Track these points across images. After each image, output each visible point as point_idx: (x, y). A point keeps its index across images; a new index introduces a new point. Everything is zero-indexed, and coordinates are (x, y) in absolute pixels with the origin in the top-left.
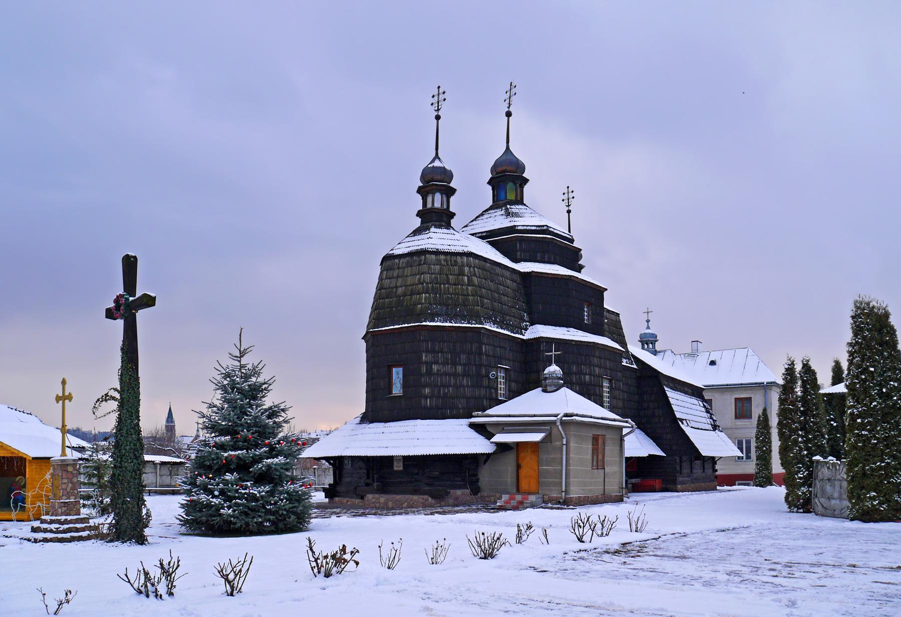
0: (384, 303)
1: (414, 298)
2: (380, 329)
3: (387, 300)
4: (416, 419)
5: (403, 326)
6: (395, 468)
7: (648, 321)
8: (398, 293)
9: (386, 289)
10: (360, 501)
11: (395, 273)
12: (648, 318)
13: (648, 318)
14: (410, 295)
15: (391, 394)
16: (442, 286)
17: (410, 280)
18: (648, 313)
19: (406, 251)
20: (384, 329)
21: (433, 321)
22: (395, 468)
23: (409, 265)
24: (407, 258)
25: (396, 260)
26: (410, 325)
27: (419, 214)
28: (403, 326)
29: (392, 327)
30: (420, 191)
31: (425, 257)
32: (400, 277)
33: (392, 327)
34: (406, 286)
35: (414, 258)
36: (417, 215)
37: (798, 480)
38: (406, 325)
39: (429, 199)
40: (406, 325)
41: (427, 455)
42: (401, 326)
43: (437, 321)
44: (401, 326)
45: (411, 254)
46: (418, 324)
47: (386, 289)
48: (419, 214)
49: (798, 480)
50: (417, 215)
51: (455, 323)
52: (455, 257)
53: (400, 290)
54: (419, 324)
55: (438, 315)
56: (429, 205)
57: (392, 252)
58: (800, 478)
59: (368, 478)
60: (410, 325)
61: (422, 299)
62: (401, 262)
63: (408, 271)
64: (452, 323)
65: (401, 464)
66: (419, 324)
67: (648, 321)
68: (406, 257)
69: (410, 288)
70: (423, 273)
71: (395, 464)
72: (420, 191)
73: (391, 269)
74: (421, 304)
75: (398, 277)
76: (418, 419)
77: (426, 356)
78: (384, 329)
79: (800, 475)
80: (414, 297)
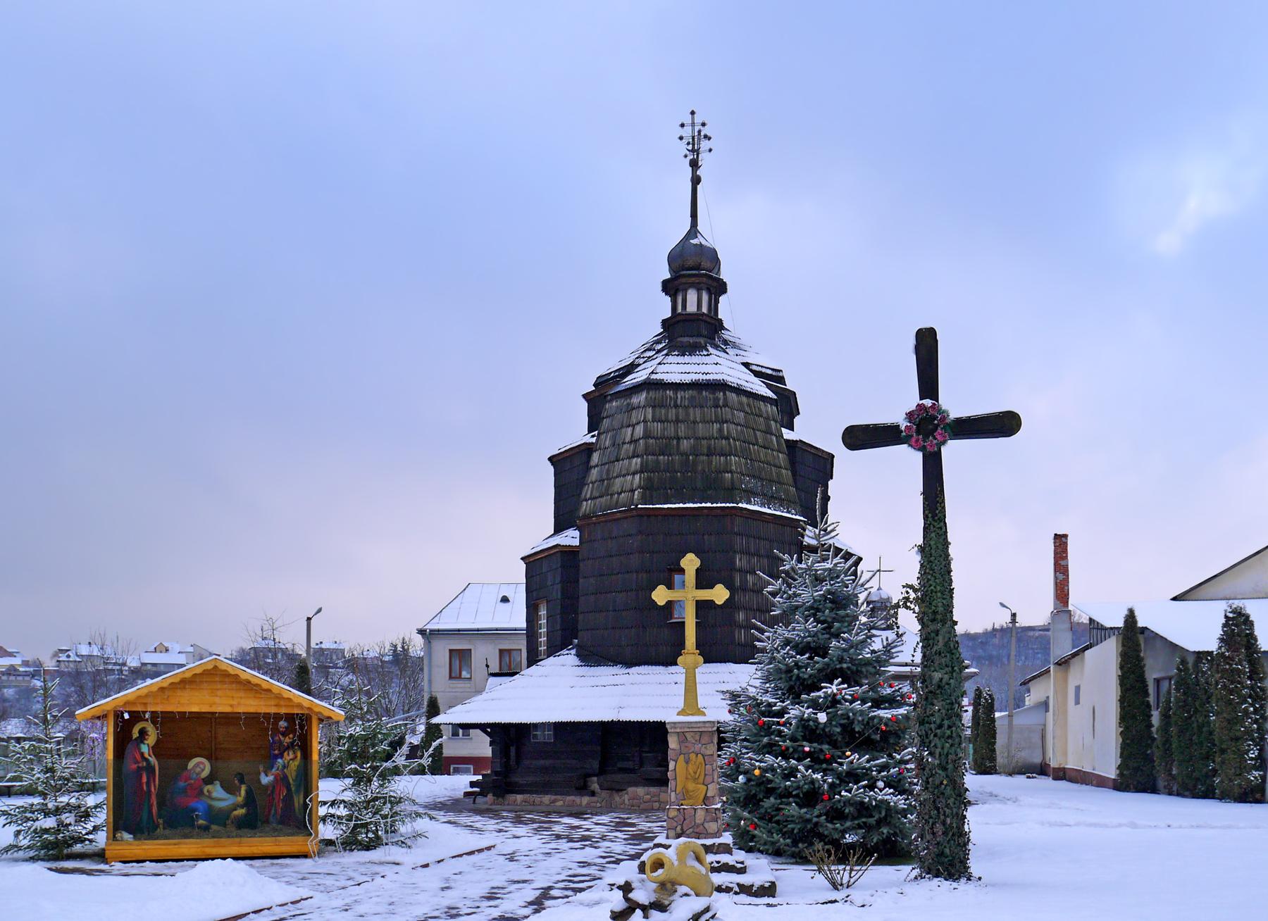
0: (657, 461)
1: (714, 460)
2: (657, 506)
3: (662, 457)
4: (725, 662)
5: (703, 505)
8: (682, 448)
9: (657, 438)
11: (672, 414)
14: (707, 455)
15: (671, 619)
16: (751, 446)
17: (701, 429)
19: (687, 379)
20: (666, 506)
21: (749, 502)
23: (694, 404)
24: (690, 392)
25: (668, 392)
26: (715, 505)
28: (703, 505)
29: (681, 505)
31: (725, 394)
32: (682, 421)
33: (681, 505)
34: (697, 438)
35: (704, 392)
37: (1249, 762)
38: (709, 505)
40: (709, 505)
41: (661, 721)
42: (699, 505)
43: (755, 504)
44: (699, 505)
45: (695, 385)
46: (732, 505)
47: (657, 438)
49: (1249, 762)
51: (775, 510)
52: (654, 392)
53: (685, 445)
54: (735, 505)
55: (755, 494)
57: (654, 377)
58: (1251, 759)
60: (715, 505)
61: (731, 465)
62: (679, 397)
63: (696, 414)
64: (770, 508)
66: (735, 505)
68: (688, 389)
69: (704, 442)
70: (726, 422)
73: (661, 406)
74: (731, 472)
75: (677, 421)
76: (729, 661)
77: (740, 560)
78: (666, 506)
79: (1251, 755)
80: (715, 459)
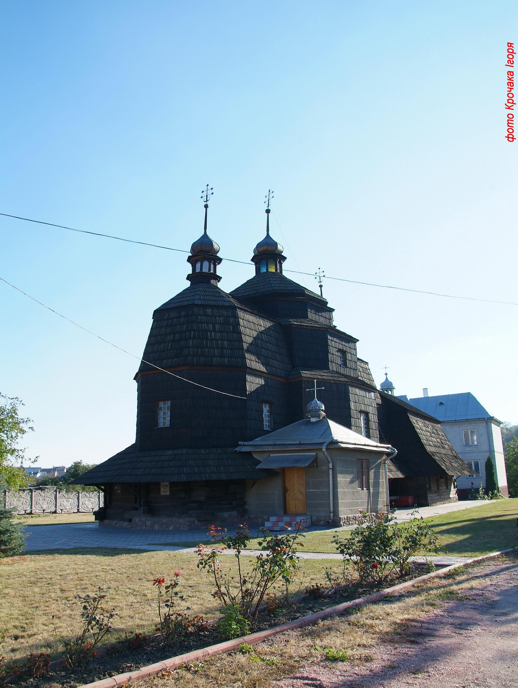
6: (162, 493)
7: (386, 374)
10: (128, 523)
12: (386, 372)
13: (386, 372)
18: (386, 368)
22: (162, 493)
27: (189, 278)
30: (189, 260)
36: (187, 279)
39: (198, 265)
48: (189, 278)
50: (187, 279)
56: (198, 270)
59: (136, 502)
65: (168, 489)
67: (386, 374)
71: (162, 489)
72: (189, 260)
